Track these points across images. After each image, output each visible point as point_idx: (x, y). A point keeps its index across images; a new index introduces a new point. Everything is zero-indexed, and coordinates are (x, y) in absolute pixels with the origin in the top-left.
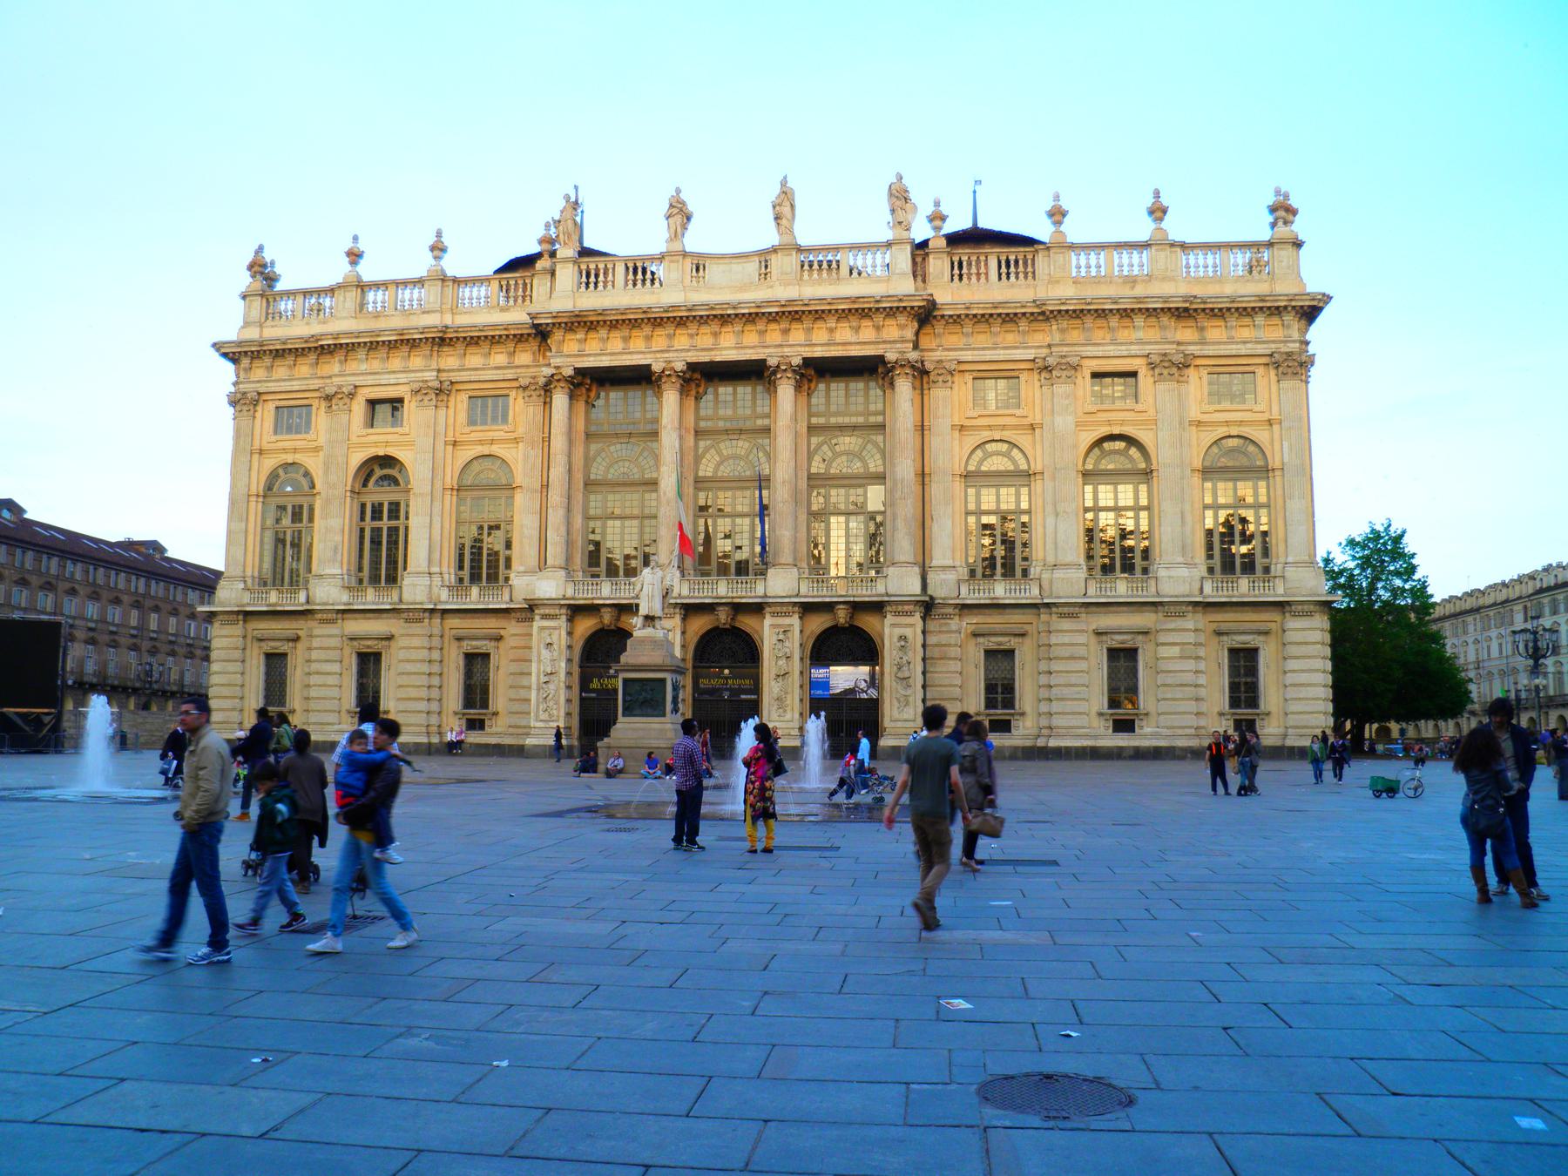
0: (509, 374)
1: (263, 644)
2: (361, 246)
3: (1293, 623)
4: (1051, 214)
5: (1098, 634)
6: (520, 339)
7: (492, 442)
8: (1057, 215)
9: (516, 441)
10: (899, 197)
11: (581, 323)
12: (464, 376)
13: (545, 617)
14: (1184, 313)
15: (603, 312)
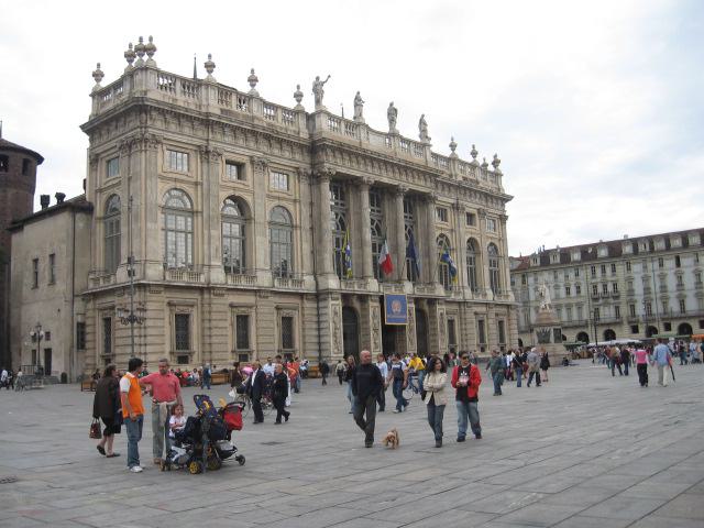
0: (294, 164)
1: (173, 308)
2: (213, 60)
3: (512, 312)
4: (451, 146)
5: (476, 314)
6: (301, 147)
7: (284, 199)
8: (453, 146)
9: (295, 201)
10: (422, 123)
11: (341, 150)
12: (273, 159)
13: (333, 299)
14: (486, 195)
15: (349, 146)
